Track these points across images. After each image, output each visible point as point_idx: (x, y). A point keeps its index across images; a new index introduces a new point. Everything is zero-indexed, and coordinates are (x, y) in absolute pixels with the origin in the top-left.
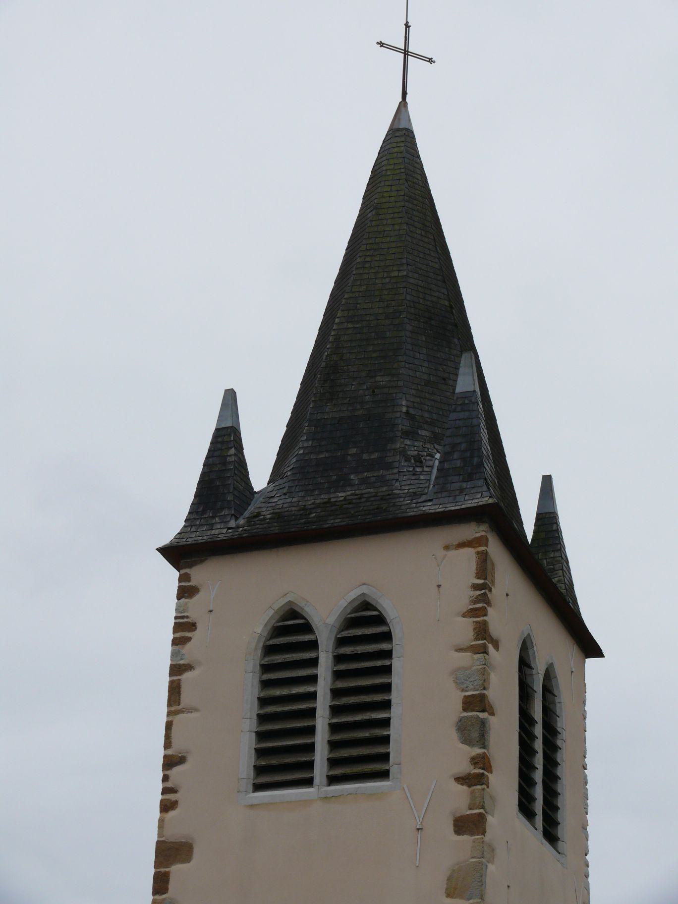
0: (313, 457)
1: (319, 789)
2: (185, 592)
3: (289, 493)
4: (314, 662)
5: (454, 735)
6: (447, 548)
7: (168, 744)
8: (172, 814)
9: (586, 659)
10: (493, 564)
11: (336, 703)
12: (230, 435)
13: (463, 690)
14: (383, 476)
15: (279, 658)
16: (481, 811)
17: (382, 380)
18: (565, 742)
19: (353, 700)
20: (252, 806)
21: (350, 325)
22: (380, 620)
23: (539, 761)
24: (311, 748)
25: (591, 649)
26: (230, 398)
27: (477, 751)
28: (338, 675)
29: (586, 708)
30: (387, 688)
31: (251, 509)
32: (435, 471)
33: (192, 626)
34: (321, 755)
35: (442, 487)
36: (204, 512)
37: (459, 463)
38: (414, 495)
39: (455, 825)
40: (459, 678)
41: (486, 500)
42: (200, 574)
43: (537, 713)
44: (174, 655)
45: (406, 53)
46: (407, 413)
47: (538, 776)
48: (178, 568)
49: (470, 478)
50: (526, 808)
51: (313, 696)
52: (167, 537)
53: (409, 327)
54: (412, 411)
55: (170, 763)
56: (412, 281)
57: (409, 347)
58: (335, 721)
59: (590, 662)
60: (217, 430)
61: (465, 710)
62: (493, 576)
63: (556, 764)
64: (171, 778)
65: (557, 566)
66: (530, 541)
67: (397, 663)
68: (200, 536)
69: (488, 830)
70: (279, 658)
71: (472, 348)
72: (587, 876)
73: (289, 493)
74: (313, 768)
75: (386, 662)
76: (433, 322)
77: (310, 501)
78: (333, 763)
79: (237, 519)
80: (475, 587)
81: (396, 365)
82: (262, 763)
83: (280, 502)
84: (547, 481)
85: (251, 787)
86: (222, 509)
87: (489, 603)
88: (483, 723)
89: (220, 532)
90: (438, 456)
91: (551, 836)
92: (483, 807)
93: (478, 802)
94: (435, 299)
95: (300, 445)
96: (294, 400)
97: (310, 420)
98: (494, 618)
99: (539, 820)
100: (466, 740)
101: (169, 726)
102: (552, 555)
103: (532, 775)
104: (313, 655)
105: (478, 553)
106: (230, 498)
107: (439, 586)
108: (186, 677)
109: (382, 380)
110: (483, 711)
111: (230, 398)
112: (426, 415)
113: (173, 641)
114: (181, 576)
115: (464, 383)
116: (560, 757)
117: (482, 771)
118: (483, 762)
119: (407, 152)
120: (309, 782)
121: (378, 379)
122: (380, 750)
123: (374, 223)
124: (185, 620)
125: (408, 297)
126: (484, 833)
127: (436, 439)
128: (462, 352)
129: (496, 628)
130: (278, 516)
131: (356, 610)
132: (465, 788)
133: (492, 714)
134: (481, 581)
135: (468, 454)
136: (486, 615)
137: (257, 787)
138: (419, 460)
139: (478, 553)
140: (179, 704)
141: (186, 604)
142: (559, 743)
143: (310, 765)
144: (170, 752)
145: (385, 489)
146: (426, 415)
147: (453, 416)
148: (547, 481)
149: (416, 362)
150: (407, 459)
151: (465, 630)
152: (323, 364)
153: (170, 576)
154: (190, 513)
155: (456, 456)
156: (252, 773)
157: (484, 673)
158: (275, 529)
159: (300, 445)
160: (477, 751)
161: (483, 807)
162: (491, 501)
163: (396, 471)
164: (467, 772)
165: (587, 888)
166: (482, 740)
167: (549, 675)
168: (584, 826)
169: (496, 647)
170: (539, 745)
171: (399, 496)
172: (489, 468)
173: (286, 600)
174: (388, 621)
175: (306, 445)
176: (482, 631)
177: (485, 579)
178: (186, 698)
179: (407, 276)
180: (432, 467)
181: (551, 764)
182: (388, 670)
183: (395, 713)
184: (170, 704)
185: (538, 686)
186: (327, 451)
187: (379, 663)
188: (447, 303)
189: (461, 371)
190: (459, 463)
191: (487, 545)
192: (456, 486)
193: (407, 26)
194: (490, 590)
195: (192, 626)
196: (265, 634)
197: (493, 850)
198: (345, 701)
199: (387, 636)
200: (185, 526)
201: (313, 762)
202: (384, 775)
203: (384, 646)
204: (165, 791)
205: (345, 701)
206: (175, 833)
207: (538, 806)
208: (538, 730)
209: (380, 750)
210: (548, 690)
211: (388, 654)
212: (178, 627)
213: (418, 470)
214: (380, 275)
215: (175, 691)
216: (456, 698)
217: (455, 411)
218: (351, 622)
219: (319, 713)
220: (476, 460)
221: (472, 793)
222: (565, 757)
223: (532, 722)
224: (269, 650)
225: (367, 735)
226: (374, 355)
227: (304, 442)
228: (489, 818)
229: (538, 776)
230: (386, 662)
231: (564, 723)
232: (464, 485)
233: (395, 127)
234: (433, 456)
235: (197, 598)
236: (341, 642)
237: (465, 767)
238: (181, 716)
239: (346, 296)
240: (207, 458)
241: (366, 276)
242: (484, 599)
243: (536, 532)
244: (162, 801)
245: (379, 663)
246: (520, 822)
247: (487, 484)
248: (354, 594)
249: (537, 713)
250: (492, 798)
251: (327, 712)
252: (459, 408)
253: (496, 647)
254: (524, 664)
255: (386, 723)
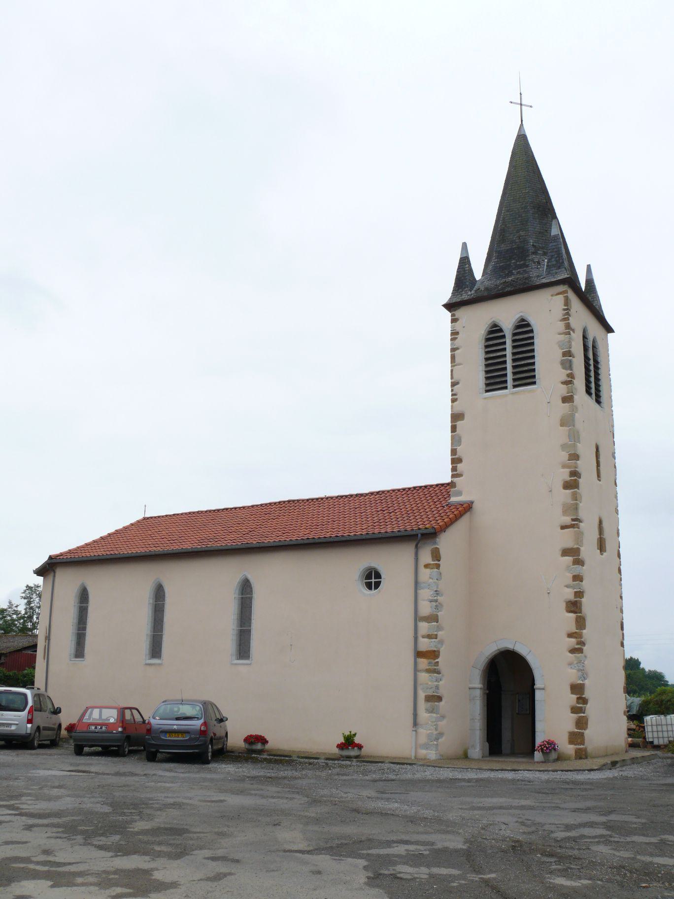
0: (498, 265)
1: (510, 390)
2: (454, 320)
3: (490, 280)
4: (505, 343)
5: (560, 366)
6: (552, 295)
7: (452, 378)
8: (455, 403)
9: (608, 334)
10: (570, 301)
11: (514, 357)
12: (466, 260)
13: (562, 349)
14: (525, 270)
15: (491, 343)
16: (572, 394)
17: (522, 233)
18: (602, 366)
19: (520, 356)
20: (485, 398)
21: (508, 213)
22: (528, 325)
23: (592, 374)
24: (506, 375)
25: (609, 329)
26: (464, 246)
27: (569, 372)
28: (514, 347)
29: (609, 353)
30: (533, 350)
31: (476, 287)
32: (545, 266)
33: (457, 333)
34: (510, 377)
35: (549, 273)
36: (458, 290)
37: (554, 263)
38: (538, 276)
39: (562, 400)
40: (560, 344)
41: (566, 276)
42: (461, 313)
43: (591, 356)
44: (452, 344)
45: (521, 105)
46: (533, 245)
47: (592, 379)
48: (450, 311)
49: (559, 268)
50: (588, 392)
51: (505, 356)
52: (445, 301)
53: (531, 212)
54: (535, 244)
55: (453, 384)
56: (531, 193)
57: (532, 219)
58: (514, 364)
59: (610, 335)
60: (461, 258)
61: (563, 357)
62: (571, 305)
63: (599, 374)
64: (454, 390)
65: (595, 299)
66: (584, 290)
67: (536, 341)
68: (458, 299)
69: (575, 401)
70: (491, 343)
71: (556, 218)
72: (612, 415)
73: (490, 280)
74: (506, 357)
75: (532, 341)
76: (540, 209)
77: (498, 282)
78: (514, 380)
79: (471, 291)
80: (564, 310)
81: (527, 227)
82: (488, 382)
83: (487, 283)
84: (589, 267)
85: (484, 392)
86: (465, 288)
87: (570, 316)
88: (570, 361)
89: (465, 297)
90: (546, 260)
91: (598, 401)
92: (572, 393)
93: (571, 391)
94: (540, 200)
95: (493, 261)
96: (489, 244)
97: (496, 251)
98: (572, 321)
99: (594, 395)
100: (565, 368)
101: (452, 371)
102: (592, 295)
103: (590, 385)
104: (504, 340)
105: (564, 296)
106: (467, 283)
107: (550, 311)
108: (457, 352)
109: (522, 233)
110: (570, 356)
111: (464, 246)
112: (540, 245)
113: (452, 469)
114: (452, 315)
115: (554, 232)
116: (600, 372)
117: (571, 379)
118: (571, 376)
119: (525, 143)
120: (506, 388)
121: (521, 233)
122: (532, 374)
123: (514, 173)
124: (454, 331)
125: (530, 200)
126: (573, 402)
127: (545, 254)
128: (552, 219)
129: (573, 325)
130: (487, 289)
131: (519, 322)
132: (565, 386)
133: (574, 357)
134: (566, 307)
135: (558, 259)
136: (569, 320)
137: (487, 391)
138: (539, 263)
139: (564, 296)
140: (455, 363)
141: (454, 325)
142: (599, 366)
143: (506, 382)
144: (453, 381)
145: (526, 275)
146: (540, 245)
147: (551, 245)
148: (589, 267)
149: (535, 225)
150: (534, 263)
151: (561, 326)
152: (499, 229)
153: (447, 315)
154: (453, 291)
155: (553, 260)
156: (484, 386)
157: (570, 342)
158: (486, 294)
159: (493, 261)
160: (569, 372)
161: (572, 393)
162: (568, 276)
163: (530, 268)
164: (565, 380)
165: (613, 420)
166: (571, 367)
167: (594, 341)
168: (611, 397)
169: (574, 332)
170: (592, 368)
171: (532, 277)
172: (566, 263)
173: (492, 320)
174: (532, 325)
175: (495, 261)
176: (568, 326)
177: (568, 306)
178: (457, 360)
179: (528, 192)
180: (544, 265)
181: (597, 374)
182: (533, 344)
183: (537, 360)
184: (451, 363)
185: (590, 346)
186: (503, 262)
187: (529, 341)
188: (545, 201)
189: (553, 227)
190: (554, 263)
191: (567, 293)
192: (554, 271)
193: (521, 94)
194: (570, 310)
195: (457, 333)
196: (485, 334)
197: (577, 408)
198: (517, 357)
199: (532, 331)
200: (452, 296)
201: (507, 380)
202: (534, 383)
203: (531, 335)
204: (452, 395)
205: (517, 357)
206: (458, 410)
207: (593, 391)
208: (592, 362)
209: (532, 374)
210: (594, 347)
211: (532, 338)
212: (452, 334)
213: (539, 266)
214: (518, 193)
215: (453, 358)
216: (560, 352)
217: (551, 242)
218: (518, 327)
219: (508, 362)
220: (561, 261)
221: (568, 388)
222: (602, 372)
223: (589, 359)
224: (487, 340)
225: (526, 369)
226: (518, 224)
227: (494, 259)
228: (575, 396)
229: (592, 379)
230: (532, 341)
231: (601, 359)
232: (557, 271)
233: (520, 134)
234: (544, 261)
235: (458, 322)
236: (514, 335)
237: (564, 378)
238: (456, 367)
239: (506, 202)
240: (458, 269)
241: (513, 194)
242: (568, 314)
243: (586, 287)
244: (452, 399)
245: (529, 341)
246: (587, 397)
247: (566, 270)
248: (518, 316)
249: (591, 356)
250: (575, 389)
251: (511, 361)
252: (553, 241)
253: (574, 332)
254: (585, 337)
255: (533, 364)
